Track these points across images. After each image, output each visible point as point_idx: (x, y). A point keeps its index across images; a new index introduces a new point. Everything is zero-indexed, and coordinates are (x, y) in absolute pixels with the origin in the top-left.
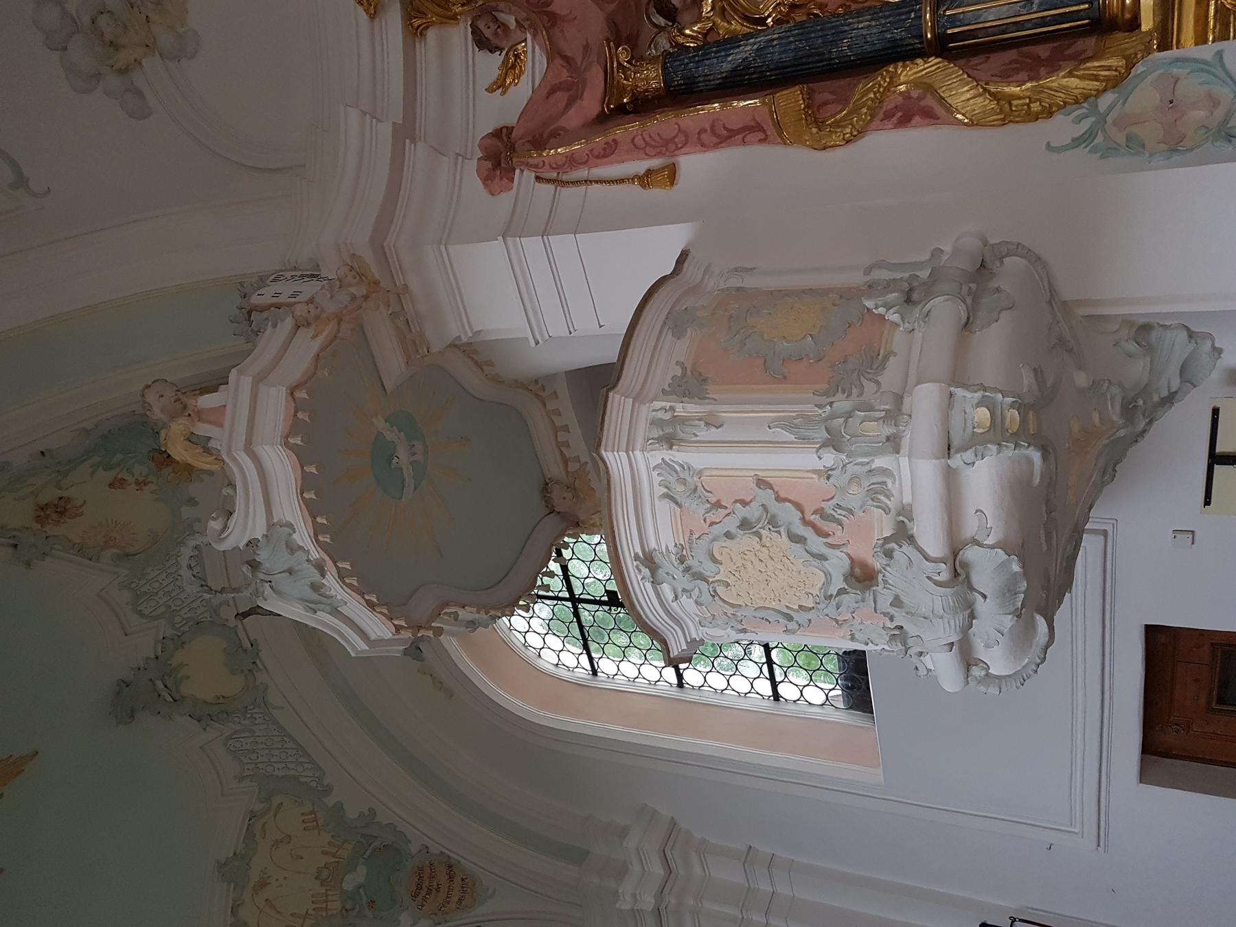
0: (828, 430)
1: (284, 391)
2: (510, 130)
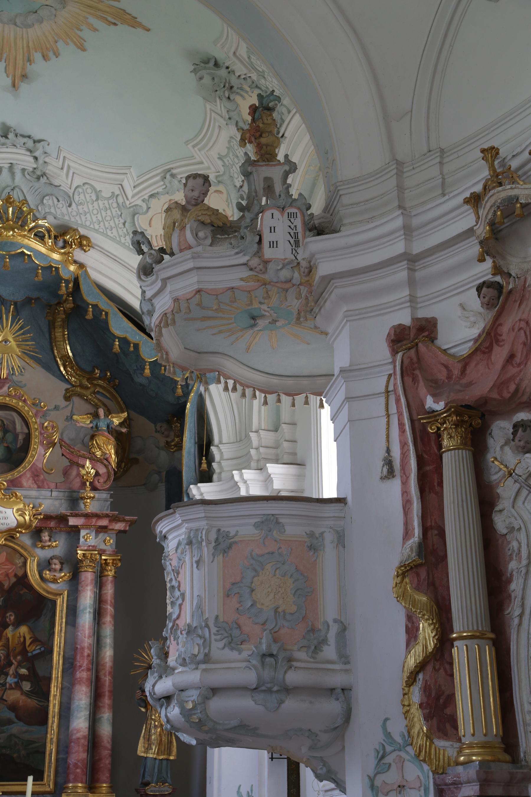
0: (196, 627)
1: (196, 287)
2: (432, 338)
